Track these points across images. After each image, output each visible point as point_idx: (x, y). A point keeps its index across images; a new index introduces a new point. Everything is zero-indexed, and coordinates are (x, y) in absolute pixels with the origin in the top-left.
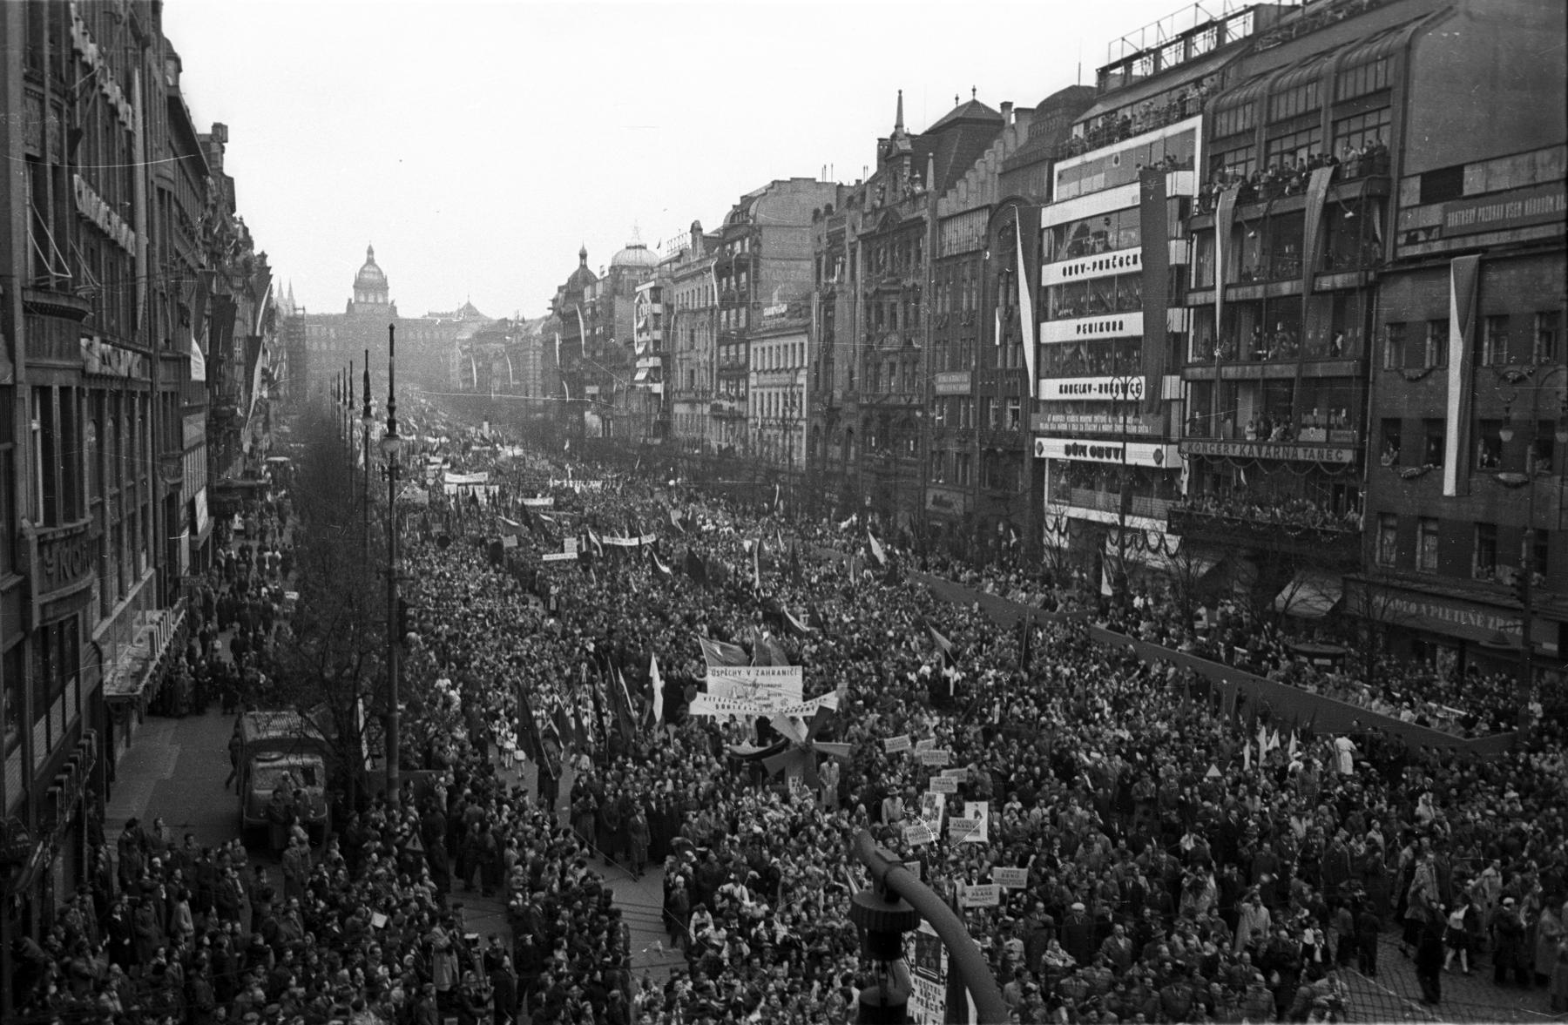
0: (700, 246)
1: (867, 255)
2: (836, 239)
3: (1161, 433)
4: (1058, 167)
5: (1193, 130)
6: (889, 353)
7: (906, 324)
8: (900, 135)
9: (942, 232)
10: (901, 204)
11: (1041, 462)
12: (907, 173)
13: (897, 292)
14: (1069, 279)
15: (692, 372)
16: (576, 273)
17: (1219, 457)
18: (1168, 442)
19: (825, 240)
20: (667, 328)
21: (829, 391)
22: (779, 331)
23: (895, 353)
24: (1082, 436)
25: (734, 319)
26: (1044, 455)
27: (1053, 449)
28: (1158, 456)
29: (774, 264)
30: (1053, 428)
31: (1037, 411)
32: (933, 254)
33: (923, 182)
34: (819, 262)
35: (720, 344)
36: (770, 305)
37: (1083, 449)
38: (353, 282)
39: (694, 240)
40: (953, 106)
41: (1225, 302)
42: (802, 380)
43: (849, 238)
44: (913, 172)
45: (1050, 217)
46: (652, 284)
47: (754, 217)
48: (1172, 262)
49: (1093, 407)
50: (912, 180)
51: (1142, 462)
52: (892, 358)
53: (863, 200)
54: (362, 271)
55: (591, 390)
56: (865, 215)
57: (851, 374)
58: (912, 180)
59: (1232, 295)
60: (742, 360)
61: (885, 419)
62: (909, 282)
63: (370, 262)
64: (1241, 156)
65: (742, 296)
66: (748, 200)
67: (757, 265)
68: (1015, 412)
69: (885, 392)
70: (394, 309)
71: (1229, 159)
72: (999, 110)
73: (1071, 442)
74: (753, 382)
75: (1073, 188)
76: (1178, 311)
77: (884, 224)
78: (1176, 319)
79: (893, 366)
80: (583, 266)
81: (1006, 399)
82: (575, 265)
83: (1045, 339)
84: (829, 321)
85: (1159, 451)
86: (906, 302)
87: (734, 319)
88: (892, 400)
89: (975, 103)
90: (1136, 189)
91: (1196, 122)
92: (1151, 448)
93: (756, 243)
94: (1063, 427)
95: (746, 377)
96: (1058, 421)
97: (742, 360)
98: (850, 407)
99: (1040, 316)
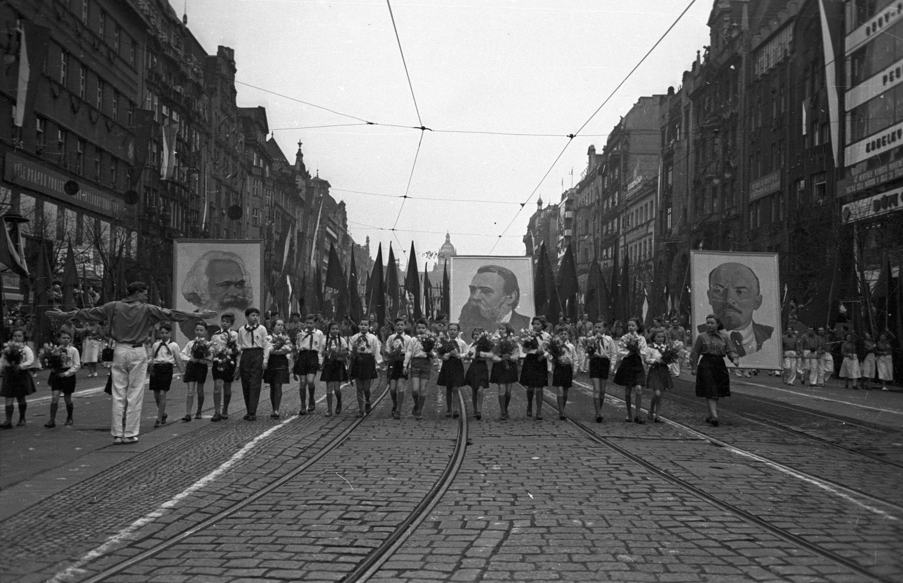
0: (593, 161)
14: (873, 35)
30: (860, 187)
33: (739, 27)
36: (631, 180)
39: (590, 158)
42: (651, 229)
47: (625, 127)
50: (730, 30)
54: (443, 248)
56: (695, 78)
62: (726, 116)
63: (448, 242)
67: (626, 159)
68: (822, 188)
69: (708, 212)
73: (879, 197)
88: (714, 219)
93: (627, 143)
94: (871, 183)
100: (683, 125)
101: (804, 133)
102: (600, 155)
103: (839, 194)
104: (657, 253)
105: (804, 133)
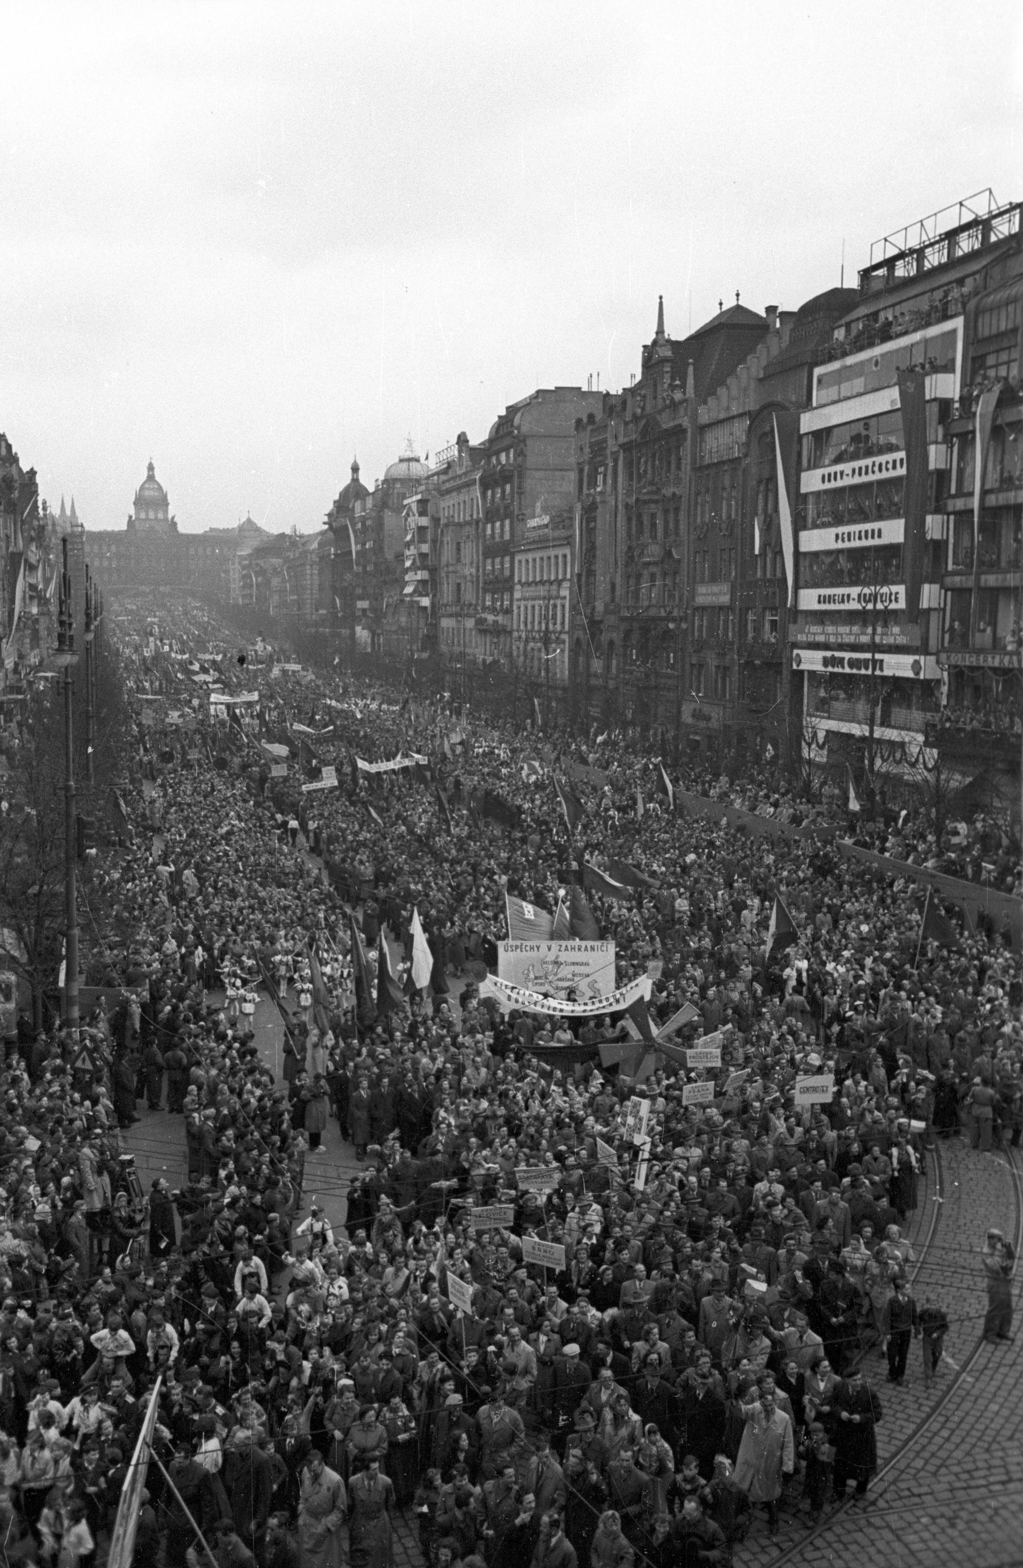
1: (629, 465)
2: (598, 449)
3: (918, 643)
4: (818, 371)
5: (954, 331)
6: (649, 564)
7: (666, 533)
8: (661, 342)
9: (702, 441)
10: (660, 412)
11: (799, 675)
12: (667, 380)
13: (656, 502)
14: (828, 486)
15: (459, 585)
16: (347, 489)
17: (979, 668)
18: (927, 653)
19: (587, 450)
20: (434, 541)
21: (590, 601)
22: (541, 543)
23: (656, 563)
24: (841, 647)
25: (500, 530)
26: (802, 667)
27: (811, 661)
28: (916, 667)
29: (538, 474)
30: (811, 639)
31: (795, 622)
32: (694, 461)
34: (581, 471)
35: (486, 556)
37: (840, 662)
38: (133, 498)
39: (460, 451)
40: (718, 312)
41: (983, 507)
42: (565, 592)
43: (612, 446)
44: (673, 379)
45: (809, 422)
46: (419, 497)
47: (518, 428)
48: (932, 466)
49: (851, 617)
50: (672, 387)
51: (900, 673)
52: (653, 569)
53: (624, 409)
54: (142, 488)
55: (363, 604)
56: (626, 424)
57: (613, 586)
58: (672, 387)
59: (992, 500)
60: (507, 573)
61: (645, 631)
62: (668, 492)
63: (151, 478)
64: (1004, 357)
65: (506, 507)
66: (512, 410)
67: (521, 476)
68: (773, 623)
69: (646, 603)
70: (174, 524)
71: (991, 360)
72: (763, 314)
73: (828, 654)
74: (517, 595)
75: (832, 393)
76: (938, 518)
77: (644, 433)
78: (934, 526)
79: (653, 576)
80: (355, 480)
81: (764, 609)
82: (347, 479)
83: (803, 548)
84: (589, 532)
85: (917, 662)
86: (666, 512)
87: (500, 530)
88: (652, 612)
89: (738, 307)
90: (895, 393)
91: (958, 323)
92: (909, 659)
93: (521, 454)
94: (821, 639)
95: (511, 590)
96: (817, 633)
97: (507, 573)
98: (612, 619)
99: (800, 524)
100: (610, 472)
101: (757, 552)
102: (473, 449)
103: (791, 639)
104: (573, 626)
105: (757, 552)
